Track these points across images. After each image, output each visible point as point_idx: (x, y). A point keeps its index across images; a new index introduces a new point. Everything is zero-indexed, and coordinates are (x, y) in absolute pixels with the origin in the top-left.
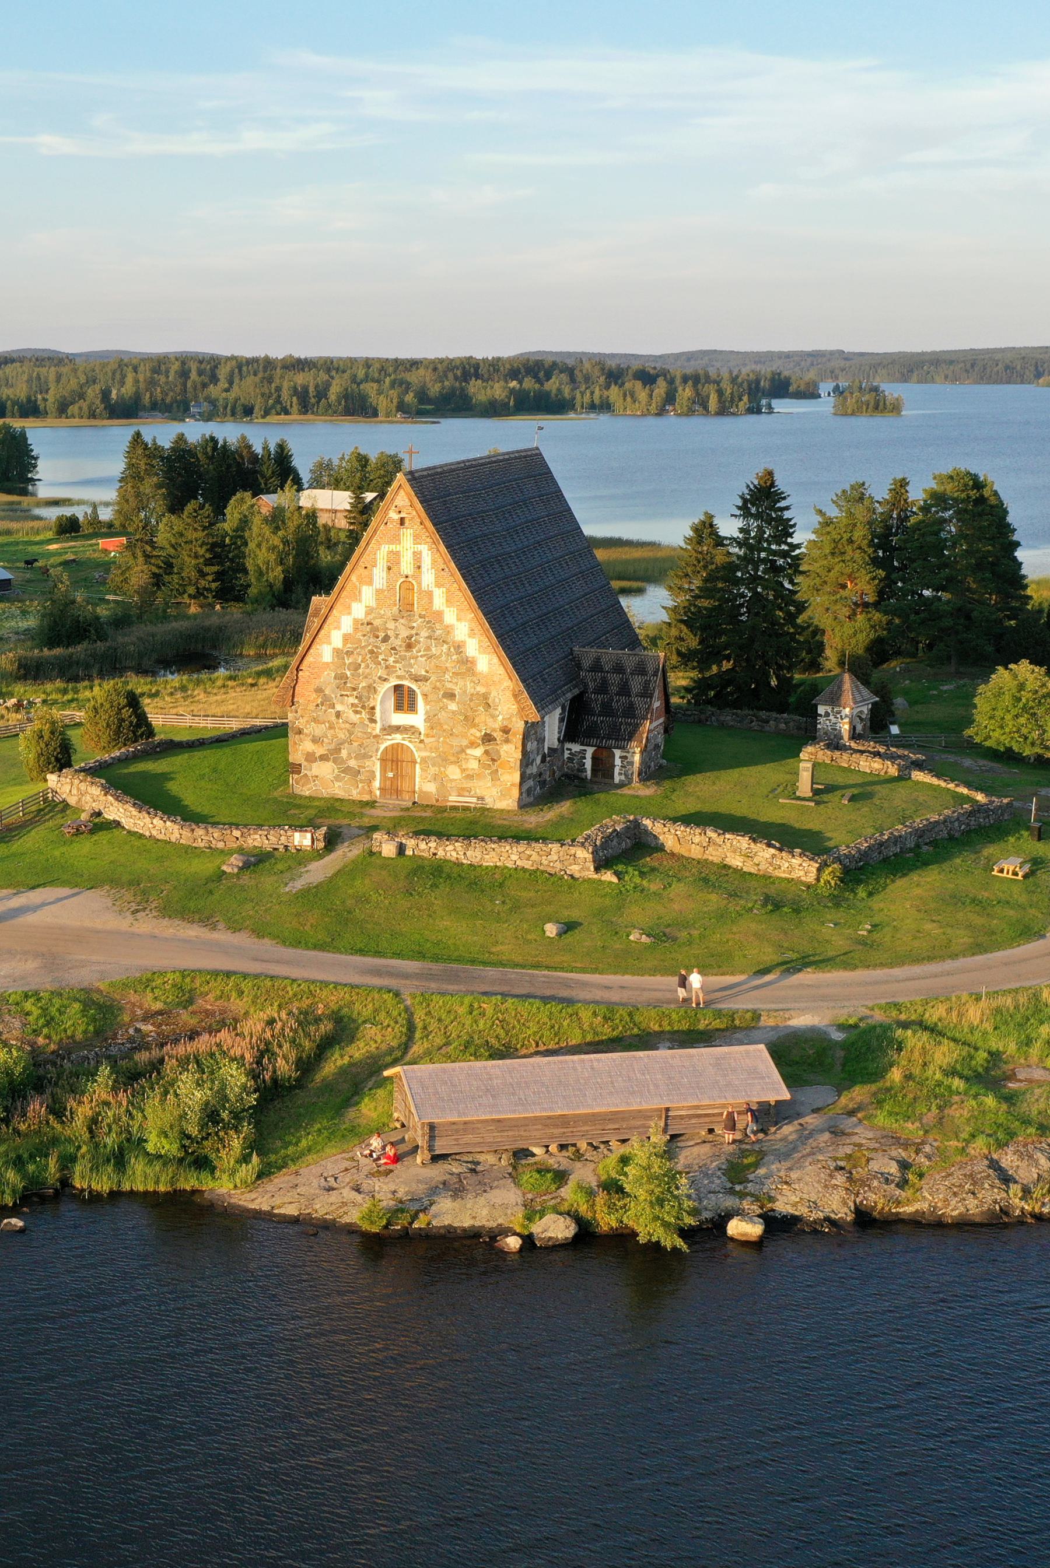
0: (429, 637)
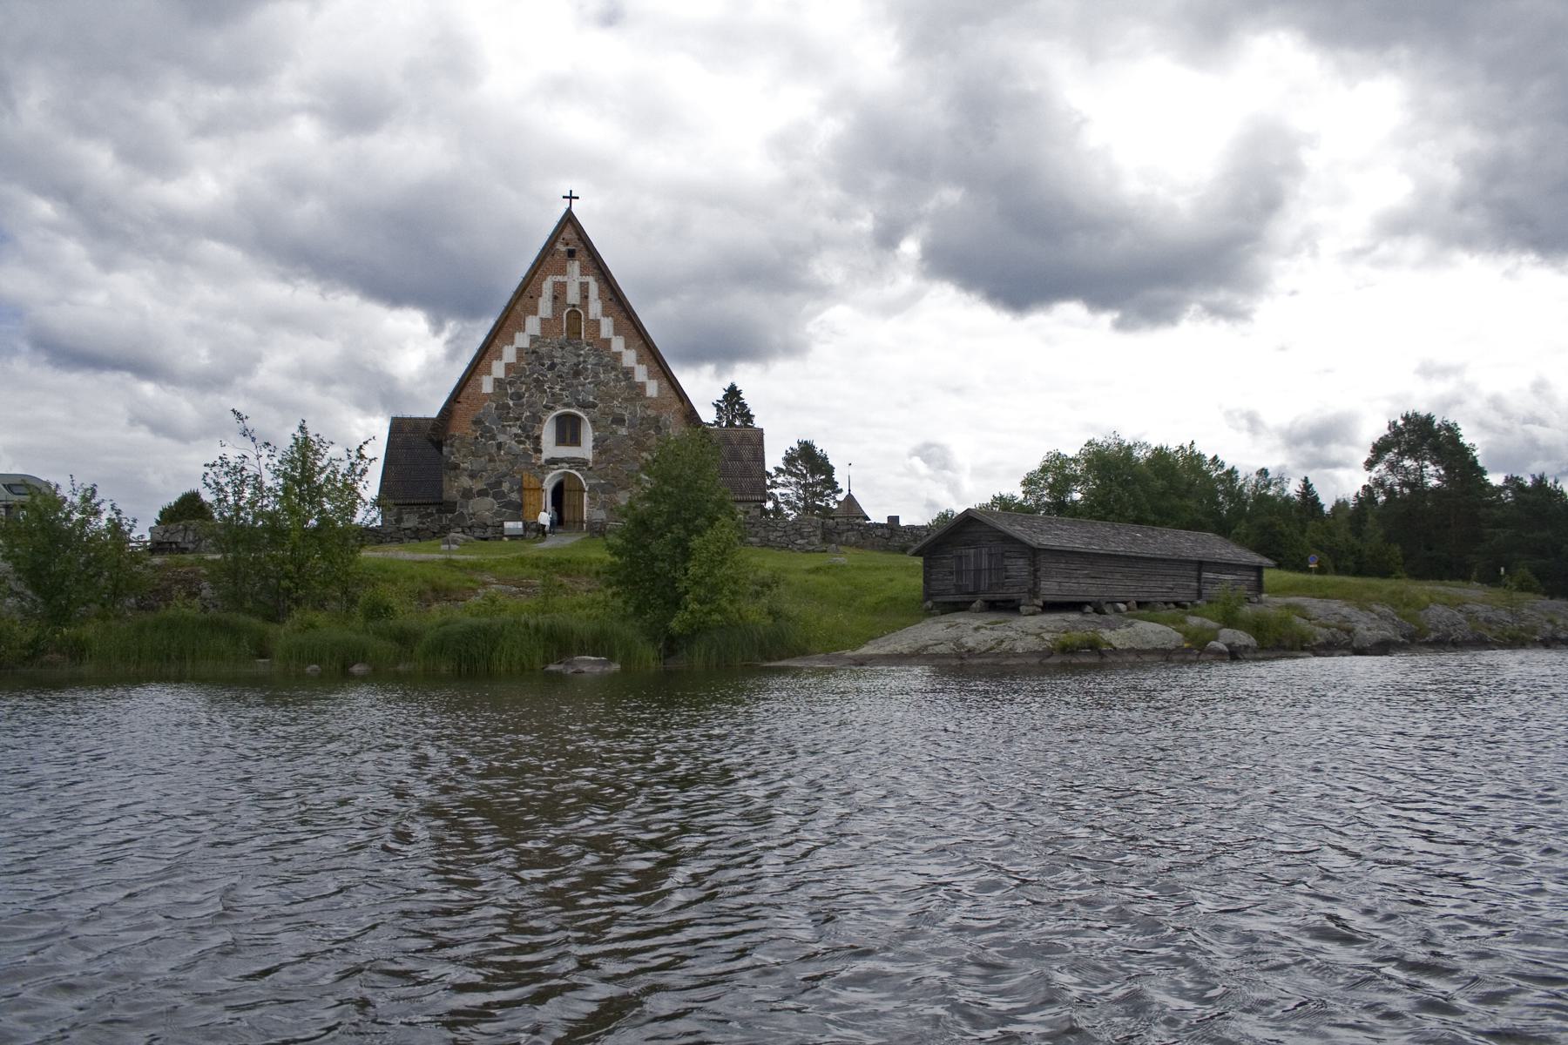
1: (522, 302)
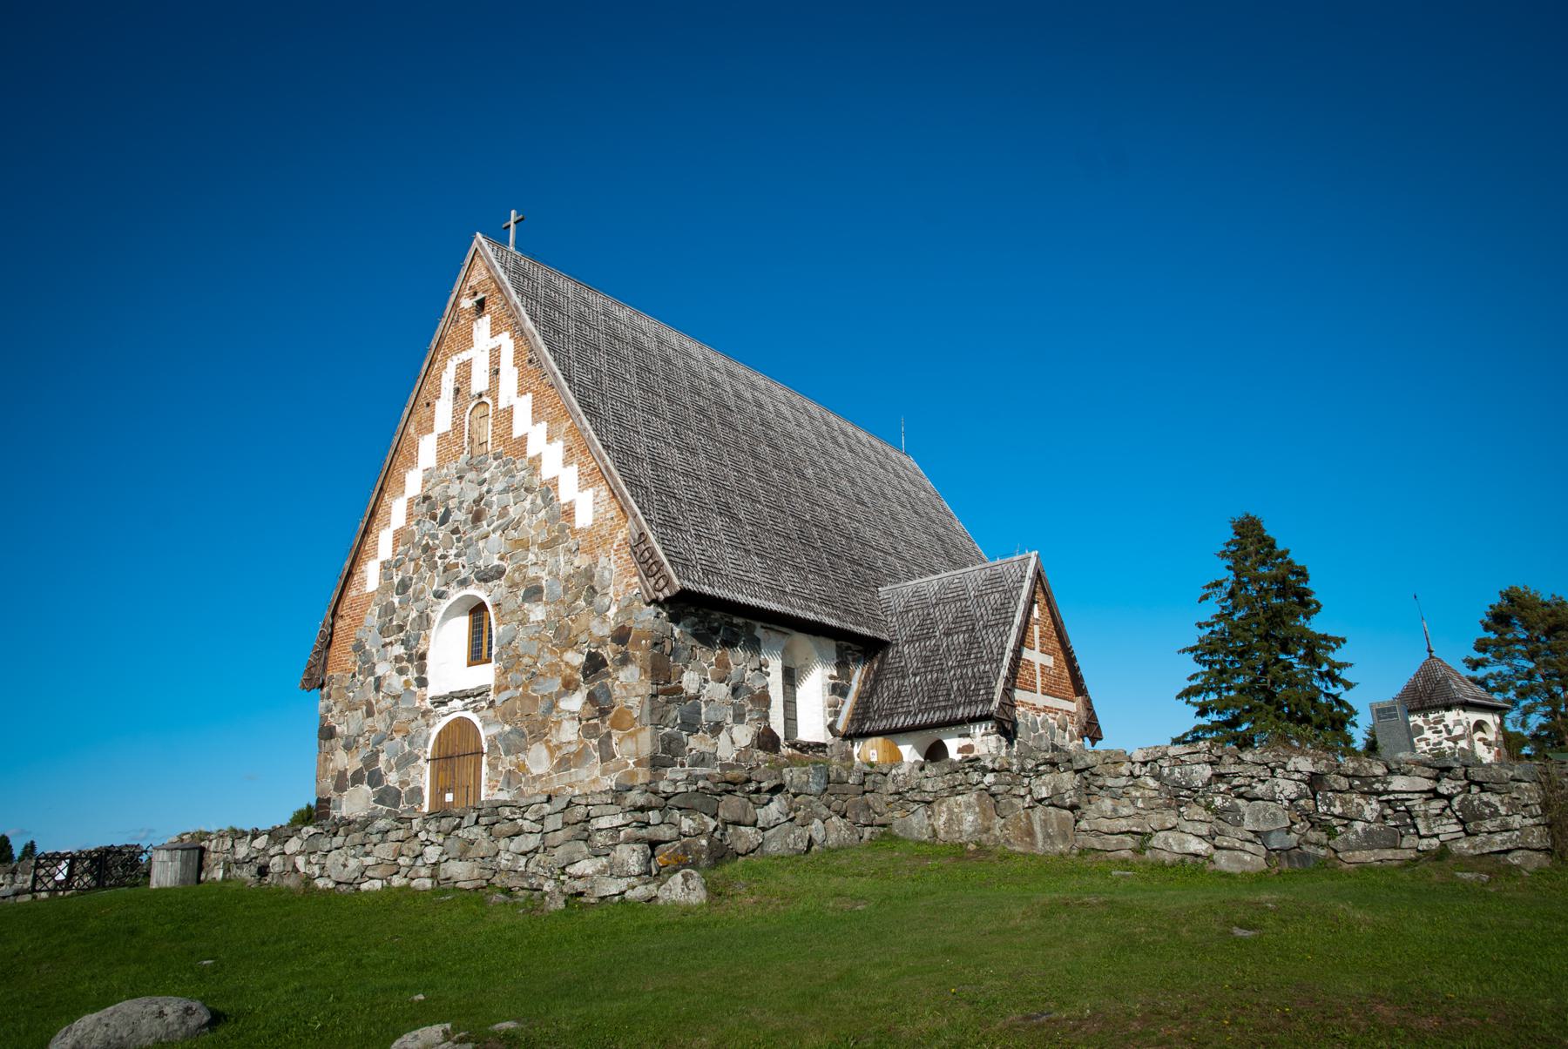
0: (505, 491)
1: (415, 418)
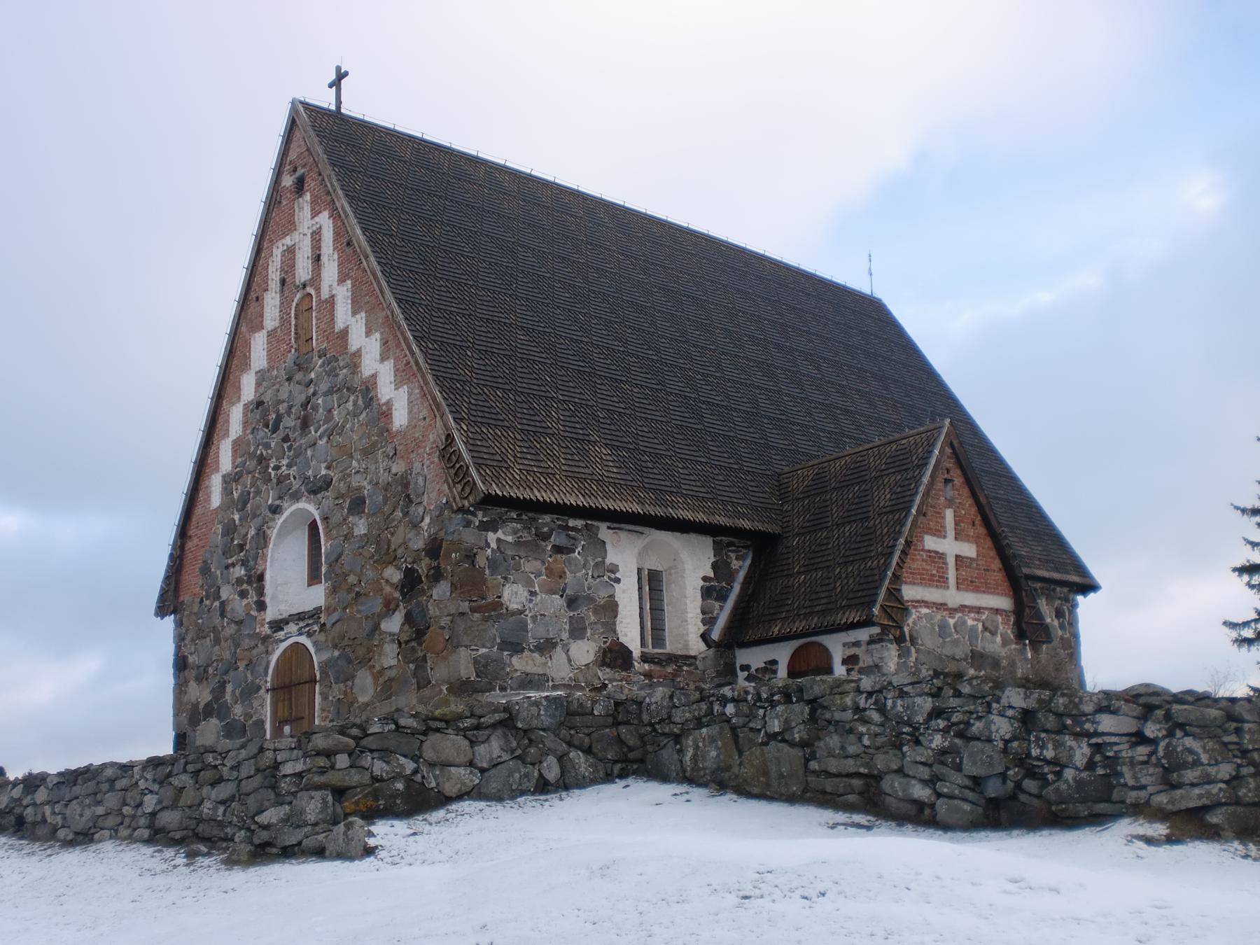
0: (330, 392)
